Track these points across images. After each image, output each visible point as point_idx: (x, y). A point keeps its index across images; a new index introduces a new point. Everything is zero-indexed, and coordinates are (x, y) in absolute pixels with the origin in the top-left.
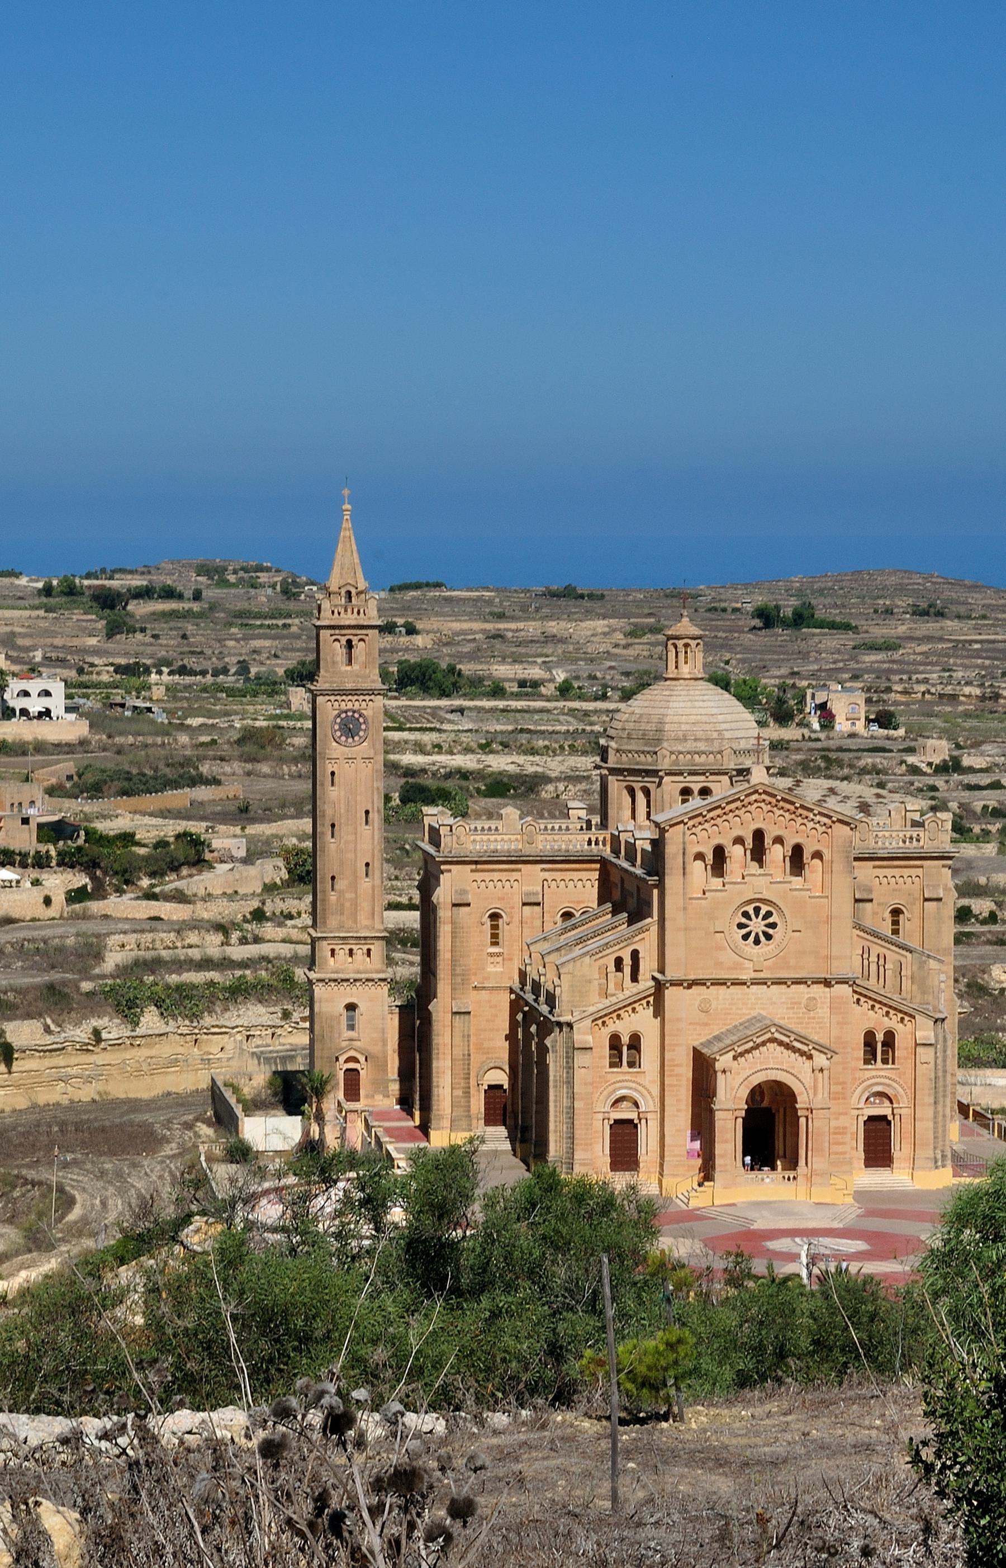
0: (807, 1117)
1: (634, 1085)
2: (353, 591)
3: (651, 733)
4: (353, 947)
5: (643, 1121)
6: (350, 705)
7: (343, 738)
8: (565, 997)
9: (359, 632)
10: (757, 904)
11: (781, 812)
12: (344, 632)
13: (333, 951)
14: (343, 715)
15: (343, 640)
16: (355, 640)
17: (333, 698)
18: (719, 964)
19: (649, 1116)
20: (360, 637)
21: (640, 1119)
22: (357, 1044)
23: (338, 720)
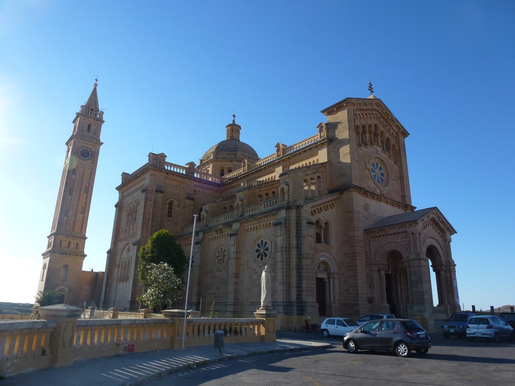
0: (445, 271)
1: (327, 255)
2: (94, 108)
3: (232, 148)
4: (71, 240)
5: (331, 280)
6: (86, 145)
7: (81, 157)
8: (291, 193)
9: (95, 121)
10: (377, 162)
11: (382, 120)
12: (90, 119)
13: (61, 241)
14: (83, 149)
15: (88, 122)
16: (93, 124)
17: (80, 140)
18: (369, 186)
19: (336, 276)
20: (95, 124)
21: (329, 278)
22: (66, 283)
23: (81, 150)
